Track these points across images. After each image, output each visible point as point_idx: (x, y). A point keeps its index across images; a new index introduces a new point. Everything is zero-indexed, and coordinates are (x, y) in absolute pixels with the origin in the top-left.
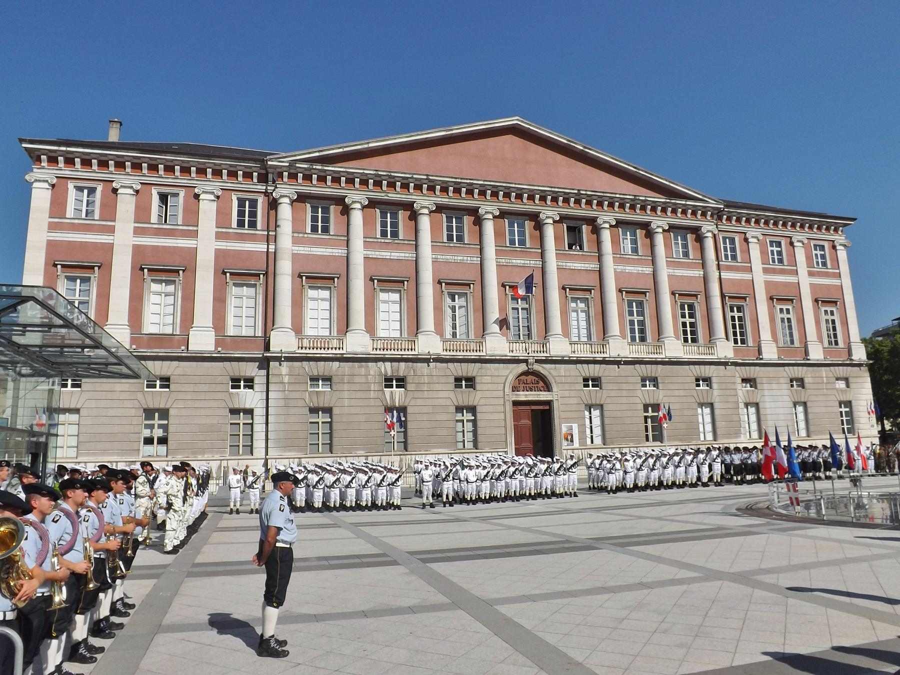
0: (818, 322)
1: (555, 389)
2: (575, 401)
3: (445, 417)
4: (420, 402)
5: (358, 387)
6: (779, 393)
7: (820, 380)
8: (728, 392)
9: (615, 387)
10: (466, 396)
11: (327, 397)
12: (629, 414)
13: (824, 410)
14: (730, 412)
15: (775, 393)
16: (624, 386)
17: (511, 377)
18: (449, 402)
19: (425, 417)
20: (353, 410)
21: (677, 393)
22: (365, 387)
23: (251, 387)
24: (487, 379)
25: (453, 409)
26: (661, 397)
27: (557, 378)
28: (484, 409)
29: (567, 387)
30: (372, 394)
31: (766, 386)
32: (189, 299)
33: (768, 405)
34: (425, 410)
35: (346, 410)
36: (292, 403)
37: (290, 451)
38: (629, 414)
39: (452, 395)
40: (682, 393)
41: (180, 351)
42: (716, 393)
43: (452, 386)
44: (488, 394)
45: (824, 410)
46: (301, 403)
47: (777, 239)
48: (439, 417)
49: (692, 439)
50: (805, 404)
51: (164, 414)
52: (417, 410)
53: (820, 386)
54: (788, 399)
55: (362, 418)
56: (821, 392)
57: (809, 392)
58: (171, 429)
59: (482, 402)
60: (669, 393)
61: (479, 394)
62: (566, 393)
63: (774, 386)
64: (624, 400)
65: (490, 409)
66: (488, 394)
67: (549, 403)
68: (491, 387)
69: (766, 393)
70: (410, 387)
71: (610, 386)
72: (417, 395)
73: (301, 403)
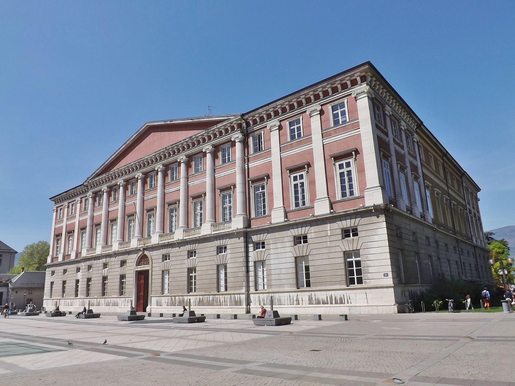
2: (158, 269)
6: (282, 250)
7: (323, 234)
8: (237, 255)
14: (236, 270)
15: (279, 251)
16: (179, 258)
21: (205, 259)
39: (118, 269)
42: (229, 256)
50: (402, 250)
52: (112, 277)
53: (324, 239)
56: (325, 245)
57: (311, 247)
59: (128, 272)
60: (201, 259)
63: (279, 245)
64: (178, 267)
69: (272, 251)
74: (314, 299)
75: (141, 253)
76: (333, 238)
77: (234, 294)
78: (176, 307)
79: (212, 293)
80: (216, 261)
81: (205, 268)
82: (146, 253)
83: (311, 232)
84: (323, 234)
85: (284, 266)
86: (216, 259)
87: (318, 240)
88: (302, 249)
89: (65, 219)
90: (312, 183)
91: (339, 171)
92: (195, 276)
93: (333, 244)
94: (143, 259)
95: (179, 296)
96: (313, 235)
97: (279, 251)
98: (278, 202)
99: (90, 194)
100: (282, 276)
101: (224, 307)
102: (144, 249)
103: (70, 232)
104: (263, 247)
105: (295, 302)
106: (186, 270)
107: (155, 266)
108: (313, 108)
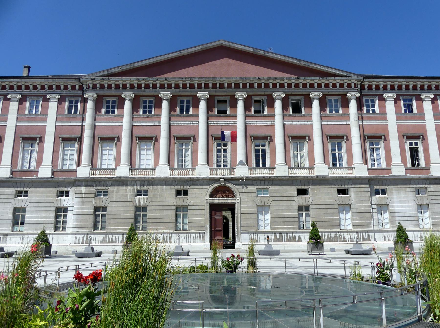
1: (238, 196)
2: (250, 203)
3: (169, 212)
4: (155, 204)
5: (120, 195)
6: (405, 198)
8: (362, 198)
9: (278, 194)
10: (181, 200)
11: (104, 201)
12: (287, 211)
14: (363, 211)
15: (402, 198)
16: (285, 194)
17: (210, 190)
18: (171, 204)
19: (157, 212)
20: (118, 208)
21: (323, 198)
22: (125, 195)
23: (68, 196)
24: (195, 191)
25: (174, 208)
26: (311, 201)
27: (239, 190)
28: (193, 207)
29: (245, 195)
30: (128, 199)
32: (41, 152)
33: (396, 206)
34: (158, 208)
35: (114, 208)
36: (86, 204)
37: (83, 229)
38: (287, 211)
39: (174, 199)
40: (326, 198)
42: (353, 198)
43: (174, 195)
44: (195, 199)
46: (90, 204)
48: (165, 212)
49: (334, 228)
51: (23, 210)
52: (153, 208)
54: (413, 202)
55: (122, 212)
58: (26, 217)
59: (192, 203)
60: (317, 198)
61: (190, 199)
62: (245, 199)
63: (402, 194)
64: (284, 203)
65: (196, 207)
66: (195, 199)
68: (197, 195)
69: (395, 198)
70: (150, 195)
71: (275, 194)
72: (153, 199)
73: (90, 204)
77: (362, 232)
78: (283, 243)
79: (335, 230)
80: (338, 202)
81: (323, 207)
85: (407, 210)
95: (287, 233)
96: (432, 189)
97: (402, 198)
101: (350, 242)
105: (419, 239)
106: (296, 207)
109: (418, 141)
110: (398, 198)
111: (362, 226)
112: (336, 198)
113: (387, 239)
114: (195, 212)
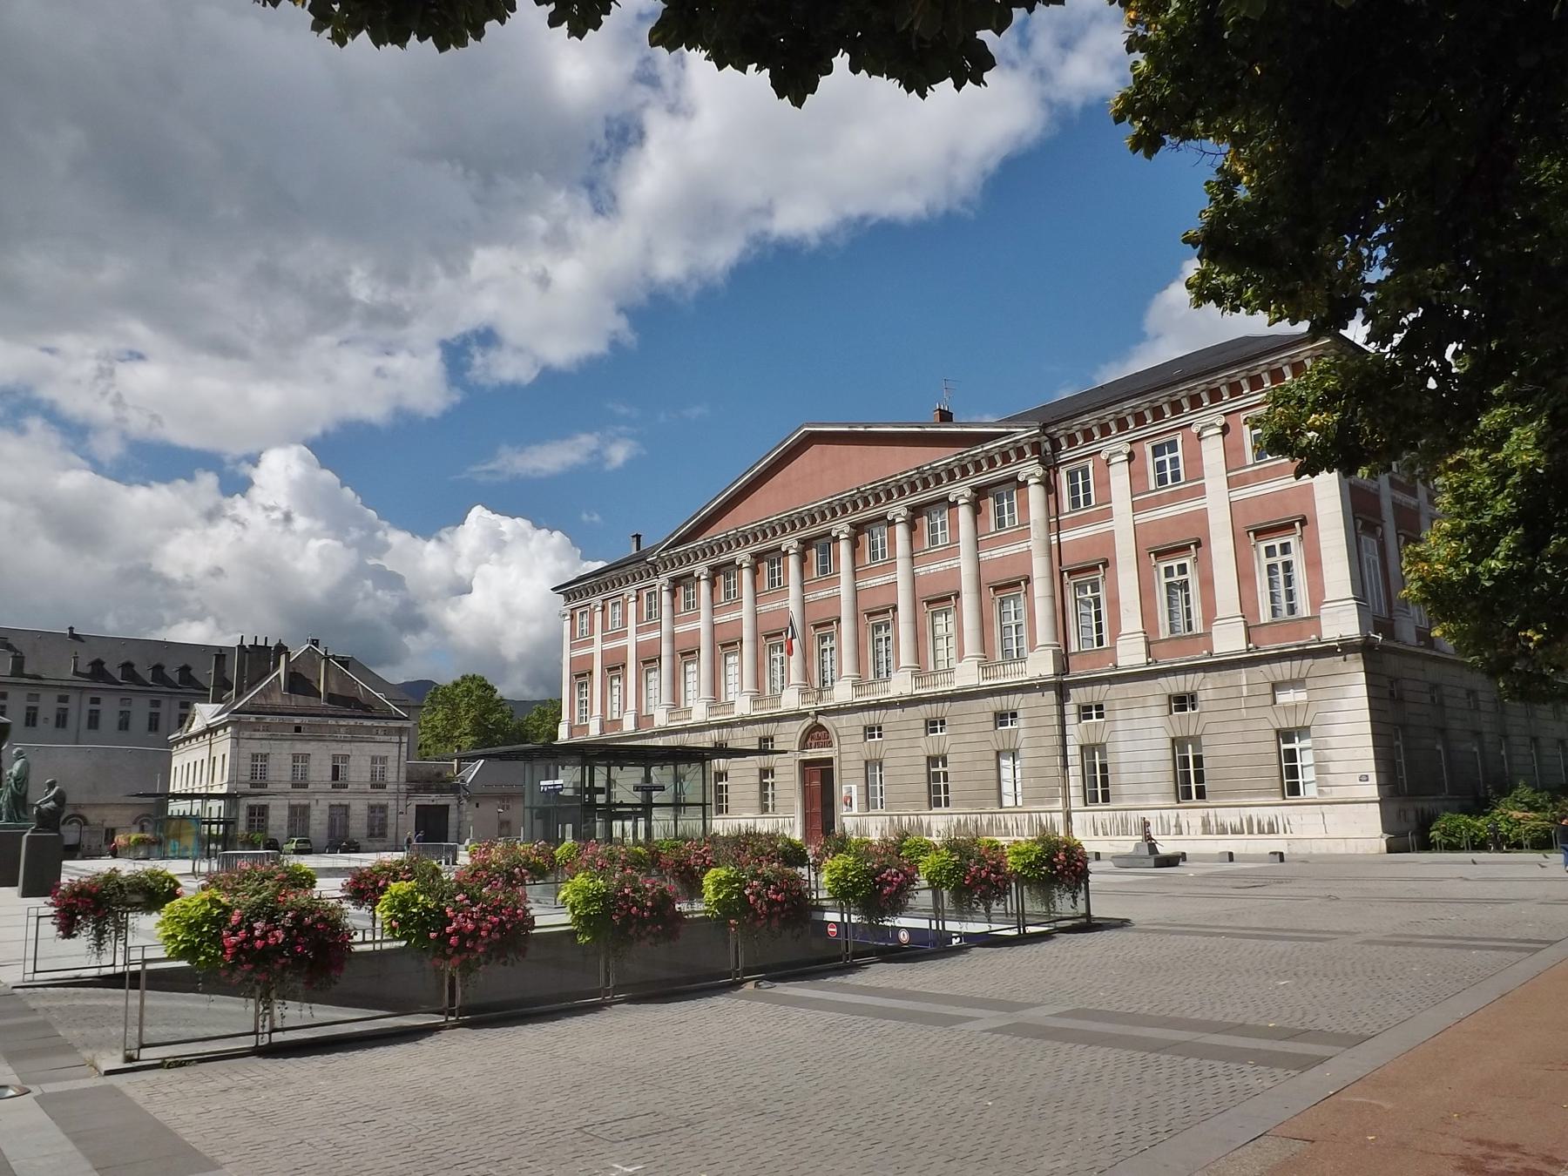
0: (1245, 577)
7: (1232, 692)
8: (1041, 732)
13: (1239, 749)
14: (1042, 762)
15: (1136, 724)
16: (906, 734)
21: (968, 738)
31: (1119, 715)
33: (1121, 747)
40: (974, 737)
41: (1310, 640)
45: (1239, 749)
47: (1165, 439)
53: (1234, 704)
54: (1161, 733)
57: (1206, 718)
60: (957, 739)
63: (1136, 713)
64: (904, 753)
67: (830, 761)
69: (1119, 725)
74: (1213, 823)
75: (809, 721)
76: (1254, 702)
79: (988, 810)
81: (968, 757)
82: (821, 720)
83: (1206, 687)
84: (1232, 692)
86: (992, 738)
87: (1223, 705)
88: (1186, 723)
89: (597, 637)
90: (1207, 583)
91: (1266, 562)
92: (945, 774)
93: (1254, 713)
94: (815, 734)
96: (1210, 694)
97: (1136, 724)
98: (1131, 621)
99: (663, 580)
100: (1144, 777)
102: (818, 713)
103: (615, 668)
104: (1100, 716)
105: (1173, 830)
107: (847, 751)
108: (1208, 420)
109: (1187, 561)
110: (1128, 725)
111: (1039, 799)
112: (991, 737)
113: (1100, 832)
114: (738, 781)
